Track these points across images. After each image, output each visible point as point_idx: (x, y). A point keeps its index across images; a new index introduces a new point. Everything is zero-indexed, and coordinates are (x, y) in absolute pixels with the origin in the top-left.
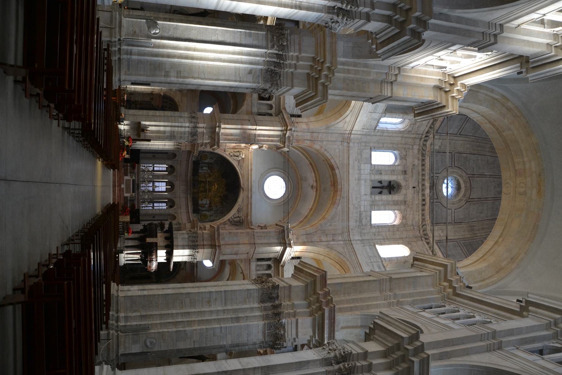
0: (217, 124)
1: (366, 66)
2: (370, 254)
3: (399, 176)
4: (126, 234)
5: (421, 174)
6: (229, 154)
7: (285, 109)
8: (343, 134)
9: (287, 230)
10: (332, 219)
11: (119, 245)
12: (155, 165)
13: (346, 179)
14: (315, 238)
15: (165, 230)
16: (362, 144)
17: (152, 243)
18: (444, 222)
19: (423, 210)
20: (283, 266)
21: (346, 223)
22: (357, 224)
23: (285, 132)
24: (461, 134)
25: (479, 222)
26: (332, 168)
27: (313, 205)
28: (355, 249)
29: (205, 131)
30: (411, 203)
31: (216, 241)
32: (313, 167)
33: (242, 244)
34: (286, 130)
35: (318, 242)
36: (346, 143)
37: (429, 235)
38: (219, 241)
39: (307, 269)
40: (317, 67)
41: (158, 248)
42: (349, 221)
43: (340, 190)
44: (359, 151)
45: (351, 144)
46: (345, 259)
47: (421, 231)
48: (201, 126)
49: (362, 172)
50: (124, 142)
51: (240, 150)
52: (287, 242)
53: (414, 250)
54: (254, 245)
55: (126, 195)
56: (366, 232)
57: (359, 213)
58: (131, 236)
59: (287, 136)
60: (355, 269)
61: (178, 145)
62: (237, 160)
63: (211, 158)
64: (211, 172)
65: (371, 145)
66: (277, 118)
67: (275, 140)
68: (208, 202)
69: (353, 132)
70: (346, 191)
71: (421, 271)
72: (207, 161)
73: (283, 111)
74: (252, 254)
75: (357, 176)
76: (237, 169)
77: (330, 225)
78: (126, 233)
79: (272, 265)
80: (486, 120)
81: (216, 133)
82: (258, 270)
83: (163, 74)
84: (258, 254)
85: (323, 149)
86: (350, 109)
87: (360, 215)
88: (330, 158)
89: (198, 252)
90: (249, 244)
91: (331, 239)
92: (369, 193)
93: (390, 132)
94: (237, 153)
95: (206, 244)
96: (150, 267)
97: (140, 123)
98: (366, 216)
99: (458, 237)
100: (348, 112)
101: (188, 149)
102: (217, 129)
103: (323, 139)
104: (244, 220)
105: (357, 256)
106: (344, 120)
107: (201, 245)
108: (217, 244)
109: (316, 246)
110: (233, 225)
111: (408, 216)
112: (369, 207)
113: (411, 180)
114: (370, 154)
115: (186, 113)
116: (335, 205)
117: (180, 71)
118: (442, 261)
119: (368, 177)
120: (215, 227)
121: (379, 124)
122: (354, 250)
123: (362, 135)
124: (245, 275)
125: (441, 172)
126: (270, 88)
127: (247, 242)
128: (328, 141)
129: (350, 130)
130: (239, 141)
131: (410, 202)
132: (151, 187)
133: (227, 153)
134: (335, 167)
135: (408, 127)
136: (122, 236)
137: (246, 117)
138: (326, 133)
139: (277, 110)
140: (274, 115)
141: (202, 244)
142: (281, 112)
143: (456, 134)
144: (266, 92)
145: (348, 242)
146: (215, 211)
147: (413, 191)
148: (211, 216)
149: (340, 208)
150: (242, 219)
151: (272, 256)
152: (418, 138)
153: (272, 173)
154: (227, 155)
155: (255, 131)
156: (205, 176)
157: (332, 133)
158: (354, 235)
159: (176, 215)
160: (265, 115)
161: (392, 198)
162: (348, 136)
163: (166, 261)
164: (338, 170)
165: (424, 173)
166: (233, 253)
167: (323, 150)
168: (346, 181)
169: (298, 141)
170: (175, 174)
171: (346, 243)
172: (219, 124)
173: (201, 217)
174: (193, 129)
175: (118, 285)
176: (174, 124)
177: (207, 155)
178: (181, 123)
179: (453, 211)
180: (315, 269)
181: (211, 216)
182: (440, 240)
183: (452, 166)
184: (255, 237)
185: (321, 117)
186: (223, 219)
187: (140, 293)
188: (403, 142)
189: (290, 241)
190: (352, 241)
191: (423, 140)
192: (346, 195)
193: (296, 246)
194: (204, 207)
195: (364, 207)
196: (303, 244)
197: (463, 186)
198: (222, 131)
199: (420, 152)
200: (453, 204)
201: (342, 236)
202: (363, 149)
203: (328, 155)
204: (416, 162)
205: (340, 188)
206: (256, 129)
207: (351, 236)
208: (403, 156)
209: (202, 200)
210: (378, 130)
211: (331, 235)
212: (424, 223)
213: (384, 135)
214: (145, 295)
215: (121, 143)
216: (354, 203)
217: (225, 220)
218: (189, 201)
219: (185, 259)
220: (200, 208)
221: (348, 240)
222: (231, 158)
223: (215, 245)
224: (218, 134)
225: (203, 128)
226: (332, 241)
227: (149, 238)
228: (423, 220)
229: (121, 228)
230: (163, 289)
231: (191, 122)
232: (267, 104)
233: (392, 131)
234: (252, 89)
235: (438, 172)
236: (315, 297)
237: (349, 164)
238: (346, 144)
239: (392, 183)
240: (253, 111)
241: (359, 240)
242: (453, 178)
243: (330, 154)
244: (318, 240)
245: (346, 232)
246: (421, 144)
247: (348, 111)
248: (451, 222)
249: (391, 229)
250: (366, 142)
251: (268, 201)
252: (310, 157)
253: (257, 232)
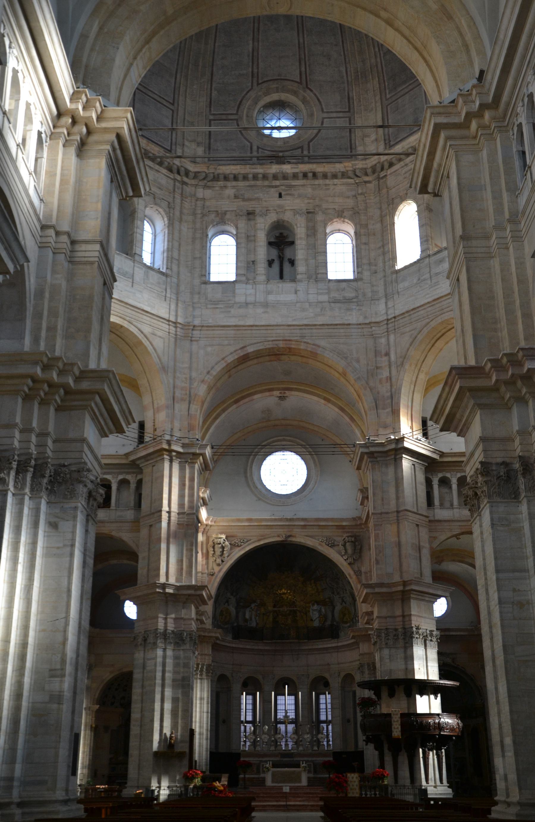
0: (158, 590)
1: (40, 293)
2: (415, 281)
3: (258, 226)
4: (386, 783)
5: (253, 183)
6: (219, 565)
7: (127, 455)
8: (176, 339)
9: (368, 447)
10: (346, 358)
11: (410, 798)
12: (243, 718)
13: (264, 332)
14: (384, 390)
15: (374, 697)
16: (196, 300)
17: (402, 725)
18: (348, 134)
19: (325, 176)
20: (442, 454)
21: (353, 330)
22: (354, 307)
23: (174, 454)
24: (171, 101)
25: (347, 60)
26: (245, 359)
27: (318, 396)
28: (404, 311)
29: (173, 616)
30: (311, 201)
31: (394, 589)
32: (243, 398)
33: (399, 537)
34: (170, 451)
35: (391, 386)
36: (194, 332)
37: (374, 163)
38: (395, 584)
39: (447, 405)
40: (44, 391)
41: (411, 711)
42: (349, 324)
43: (288, 342)
44: (209, 306)
45: (197, 322)
46: (425, 331)
47: (366, 179)
48: (163, 625)
49: (251, 299)
50: (195, 787)
51: (211, 543)
52: (393, 446)
53: (405, 192)
54: (401, 514)
55: (304, 782)
56: (370, 290)
57: (332, 305)
58: (389, 769)
59: (181, 450)
60: (445, 310)
61: (202, 671)
62: (231, 549)
63: (227, 602)
65: (197, 281)
66: (147, 471)
67: (190, 473)
68: (316, 607)
69: (173, 319)
70: (289, 331)
71: (448, 177)
72: (233, 610)
73: (132, 458)
74: (418, 516)
75: (260, 310)
76: (247, 549)
77: (358, 361)
78: (383, 782)
79: (440, 475)
80: (144, 50)
81: (176, 592)
82: (452, 505)
83: (55, 706)
84: (419, 505)
85: (206, 378)
86: (125, 324)
87: (336, 301)
88: (225, 365)
89: (418, 628)
90: (398, 523)
91: (385, 359)
92: (293, 285)
93: (170, 244)
94: (216, 550)
95: (401, 611)
96: (452, 729)
97: (156, 754)
98: (338, 290)
99: (379, 104)
100: (132, 329)
101: (208, 650)
102: (169, 591)
103: (186, 378)
104: (350, 534)
105: (418, 307)
106: (148, 336)
107: (404, 622)
108: (400, 588)
109: (400, 389)
110: (360, 557)
111: (336, 207)
112: (321, 285)
113: (266, 201)
114: (216, 285)
115: (137, 655)
116: (319, 352)
117: (51, 670)
118: (427, 134)
119: (261, 287)
120: (366, 593)
121: (156, 266)
122: (407, 312)
123: (177, 300)
124: (463, 530)
125: (249, 142)
126: (86, 486)
127: (395, 527)
128: (190, 368)
129: (169, 325)
130: (192, 545)
131: (309, 203)
132: (286, 727)
133: (217, 569)
134: (242, 354)
135: (160, 210)
136: (390, 792)
137: (144, 532)
138: (175, 372)
139: (130, 470)
140: (139, 477)
141: (401, 619)
142: (134, 461)
143: (173, 111)
144: (94, 494)
145: (390, 326)
146: (333, 593)
147: (288, 197)
148: (343, 601)
149: (322, 343)
150: (348, 537)
151: (421, 477)
152: (182, 189)
153: (255, 478)
155: (173, 514)
156: (264, 614)
157: (175, 361)
158: (376, 314)
159: (343, 674)
160: (140, 495)
161: (301, 238)
162: (181, 328)
163: (439, 695)
164: (248, 348)
165: (250, 176)
166: (418, 555)
167: (209, 378)
168: (269, 331)
169: (191, 428)
170: (260, 677)
171: (393, 328)
172: (158, 587)
173: (346, 623)
174: (168, 641)
175: (496, 803)
176: (159, 681)
177: (222, 611)
178: (155, 665)
179: (325, 115)
180: (447, 389)
181: (343, 601)
182: (385, 140)
183: (237, 120)
184: (383, 511)
185: (142, 382)
186: (350, 575)
187: (510, 754)
188: (190, 218)
189: (391, 441)
190: (389, 317)
191: (185, 179)
192: (298, 331)
193: (400, 428)
195: (321, 294)
196: (396, 414)
197: (275, 97)
198: (172, 580)
199: (209, 184)
200: (312, 115)
201: (379, 337)
202: (206, 298)
203: (218, 368)
204: (230, 192)
205: (284, 342)
206: (169, 512)
207: (378, 320)
208: (217, 219)
209: (312, 620)
210: (167, 268)
211: (379, 359)
212: (351, 174)
213: (177, 258)
214: (514, 742)
215: (197, 794)
216: (312, 315)
217: (352, 573)
218: (314, 647)
219: (433, 654)
220: (328, 623)
221: (387, 324)
222: (228, 561)
223: (403, 592)
224: (177, 588)
225: (166, 619)
226: (390, 358)
227: (391, 732)
228: (344, 175)
229: (373, 793)
230: (498, 702)
231: (155, 644)
232: (118, 489)
233: (168, 241)
234: (87, 521)
235: (249, 149)
236: (503, 389)
237: (235, 326)
238: (196, 333)
239: (272, 240)
240: (132, 517)
241: (386, 303)
242: (260, 117)
243: (216, 364)
244: (389, 384)
245: (370, 330)
246: (193, 182)
247: (131, 329)
248: (348, 119)
249: (364, 239)
250: (192, 293)
251: (311, 486)
252: (223, 402)
253: (374, 508)
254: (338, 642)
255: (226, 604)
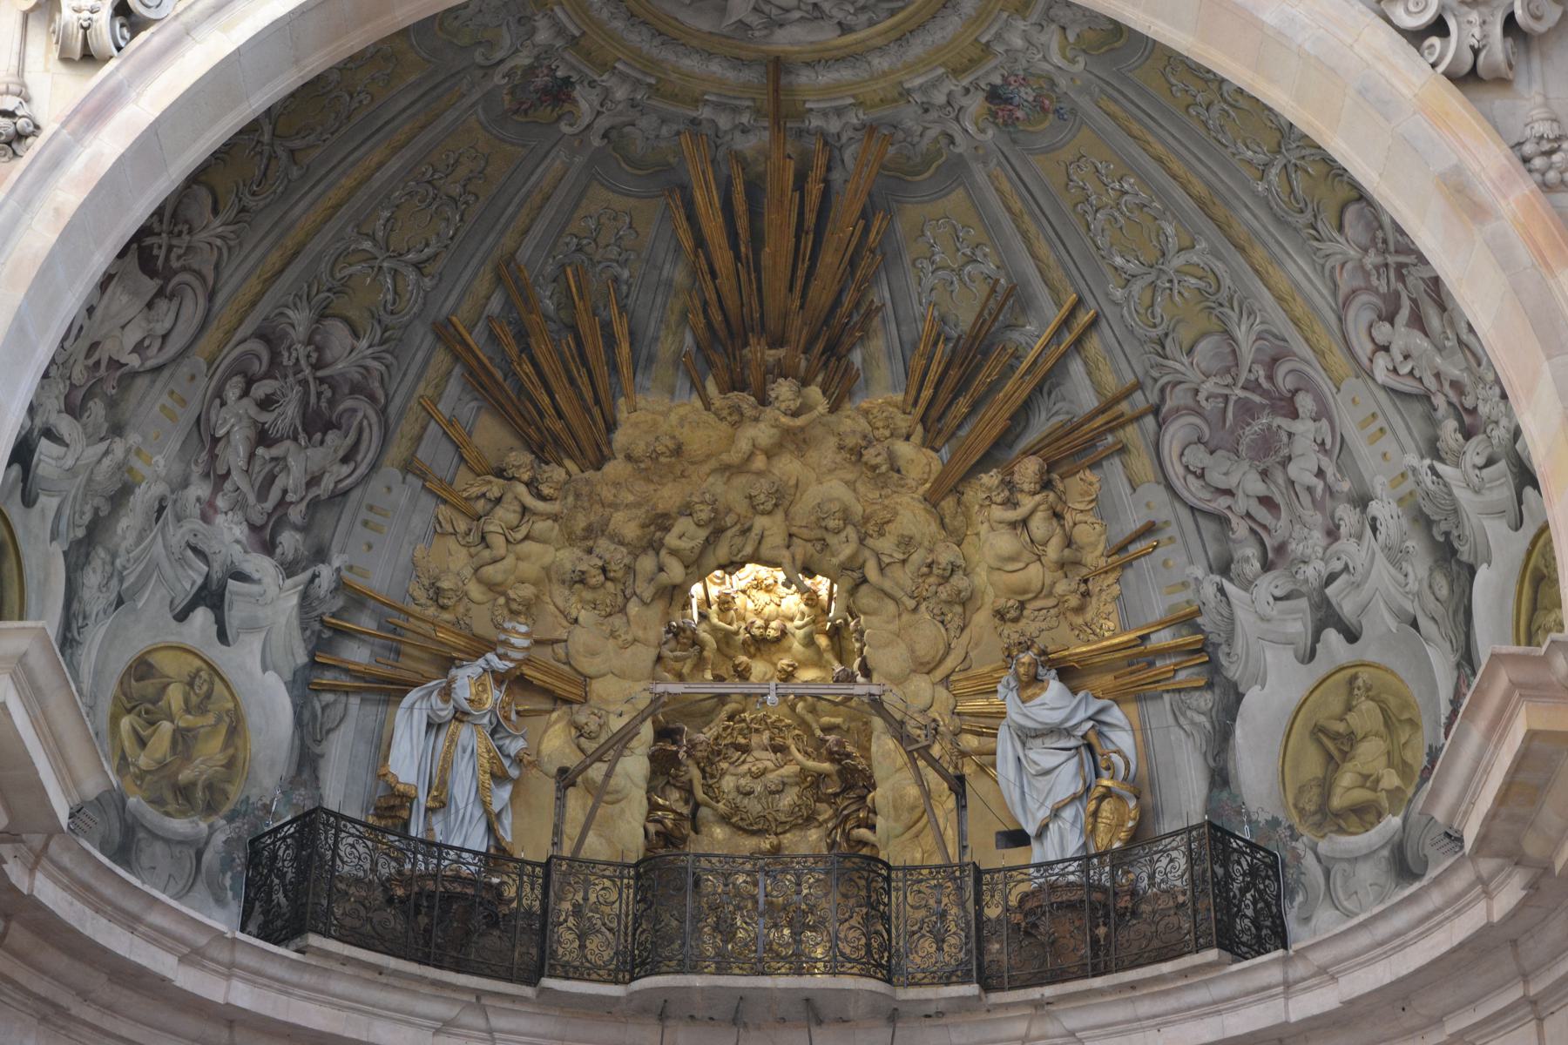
63: (211, 596)
64: (480, 646)
146: (1224, 567)
148: (1326, 617)
154: (94, 114)
156: (566, 779)
173: (1364, 814)
177: (142, 668)
194: (1142, 787)
254: (1288, 986)
255: (202, 617)
